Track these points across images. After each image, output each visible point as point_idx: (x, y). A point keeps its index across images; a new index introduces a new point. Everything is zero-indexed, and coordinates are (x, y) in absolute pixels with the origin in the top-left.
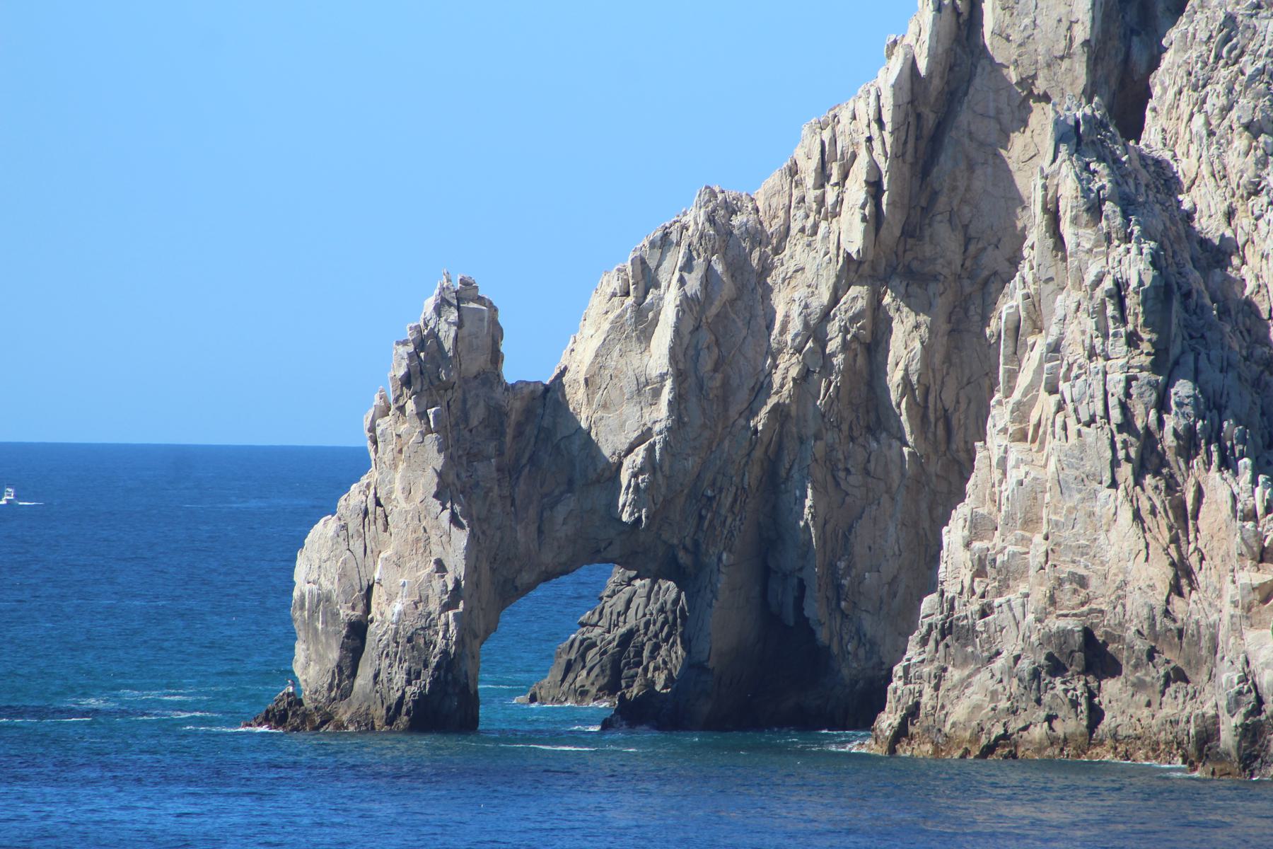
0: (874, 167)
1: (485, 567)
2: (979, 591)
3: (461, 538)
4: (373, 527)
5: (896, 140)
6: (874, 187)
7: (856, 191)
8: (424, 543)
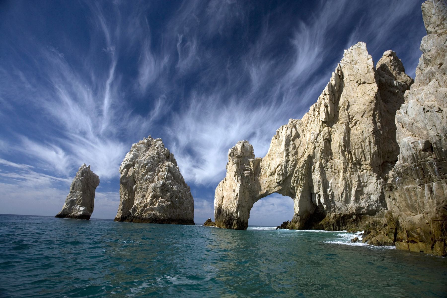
0: (325, 103)
1: (247, 193)
3: (239, 185)
5: (330, 97)
6: (326, 107)
8: (231, 186)
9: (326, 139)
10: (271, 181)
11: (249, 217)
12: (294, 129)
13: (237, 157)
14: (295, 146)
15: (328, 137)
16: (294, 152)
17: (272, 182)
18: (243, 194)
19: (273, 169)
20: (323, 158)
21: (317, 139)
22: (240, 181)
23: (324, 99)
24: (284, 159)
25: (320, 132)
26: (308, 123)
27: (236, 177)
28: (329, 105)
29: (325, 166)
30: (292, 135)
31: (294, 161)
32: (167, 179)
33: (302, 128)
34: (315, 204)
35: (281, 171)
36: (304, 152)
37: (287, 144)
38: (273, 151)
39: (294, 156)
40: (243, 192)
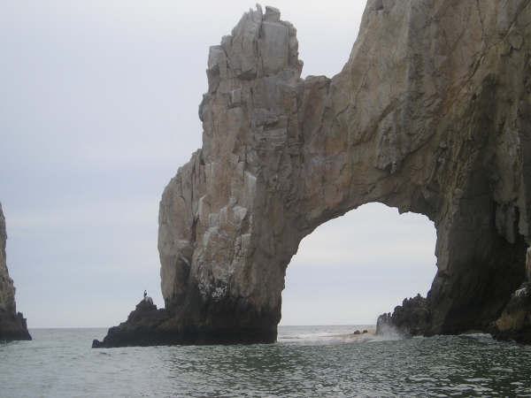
4: (198, 180)
10: (360, 163)
11: (295, 253)
19: (365, 121)
21: (515, 20)
24: (404, 88)
31: (436, 96)
34: (503, 239)
36: (475, 67)
39: (439, 82)
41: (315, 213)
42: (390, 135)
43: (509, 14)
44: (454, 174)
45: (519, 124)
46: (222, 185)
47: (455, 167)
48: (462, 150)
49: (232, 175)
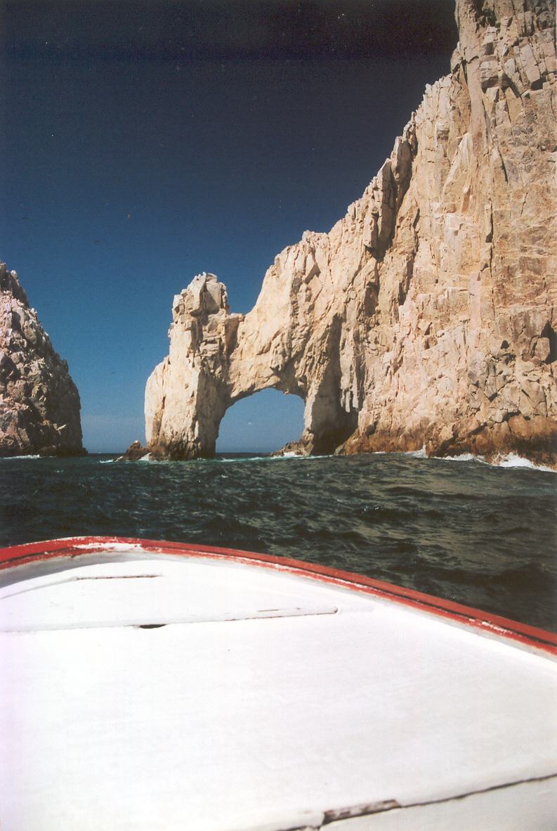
1: (213, 389)
2: (424, 329)
3: (196, 373)
5: (385, 195)
6: (376, 216)
7: (369, 218)
9: (370, 284)
10: (261, 365)
11: (217, 436)
12: (310, 256)
13: (193, 314)
14: (311, 295)
15: (373, 280)
16: (307, 307)
17: (263, 368)
18: (205, 392)
19: (265, 342)
20: (361, 321)
21: (352, 282)
22: (198, 367)
23: (373, 197)
24: (287, 321)
25: (360, 268)
26: (340, 243)
27: (191, 355)
28: (380, 214)
29: (364, 338)
30: (305, 271)
31: (306, 325)
32: (13, 347)
33: (327, 254)
35: (281, 346)
36: (328, 308)
37: (295, 289)
38: (267, 302)
39: (308, 317)
40: (205, 388)
41: (234, 394)
42: (278, 348)
43: (348, 279)
44: (315, 372)
45: (353, 342)
46: (180, 376)
47: (316, 368)
48: (320, 358)
49: (186, 370)
